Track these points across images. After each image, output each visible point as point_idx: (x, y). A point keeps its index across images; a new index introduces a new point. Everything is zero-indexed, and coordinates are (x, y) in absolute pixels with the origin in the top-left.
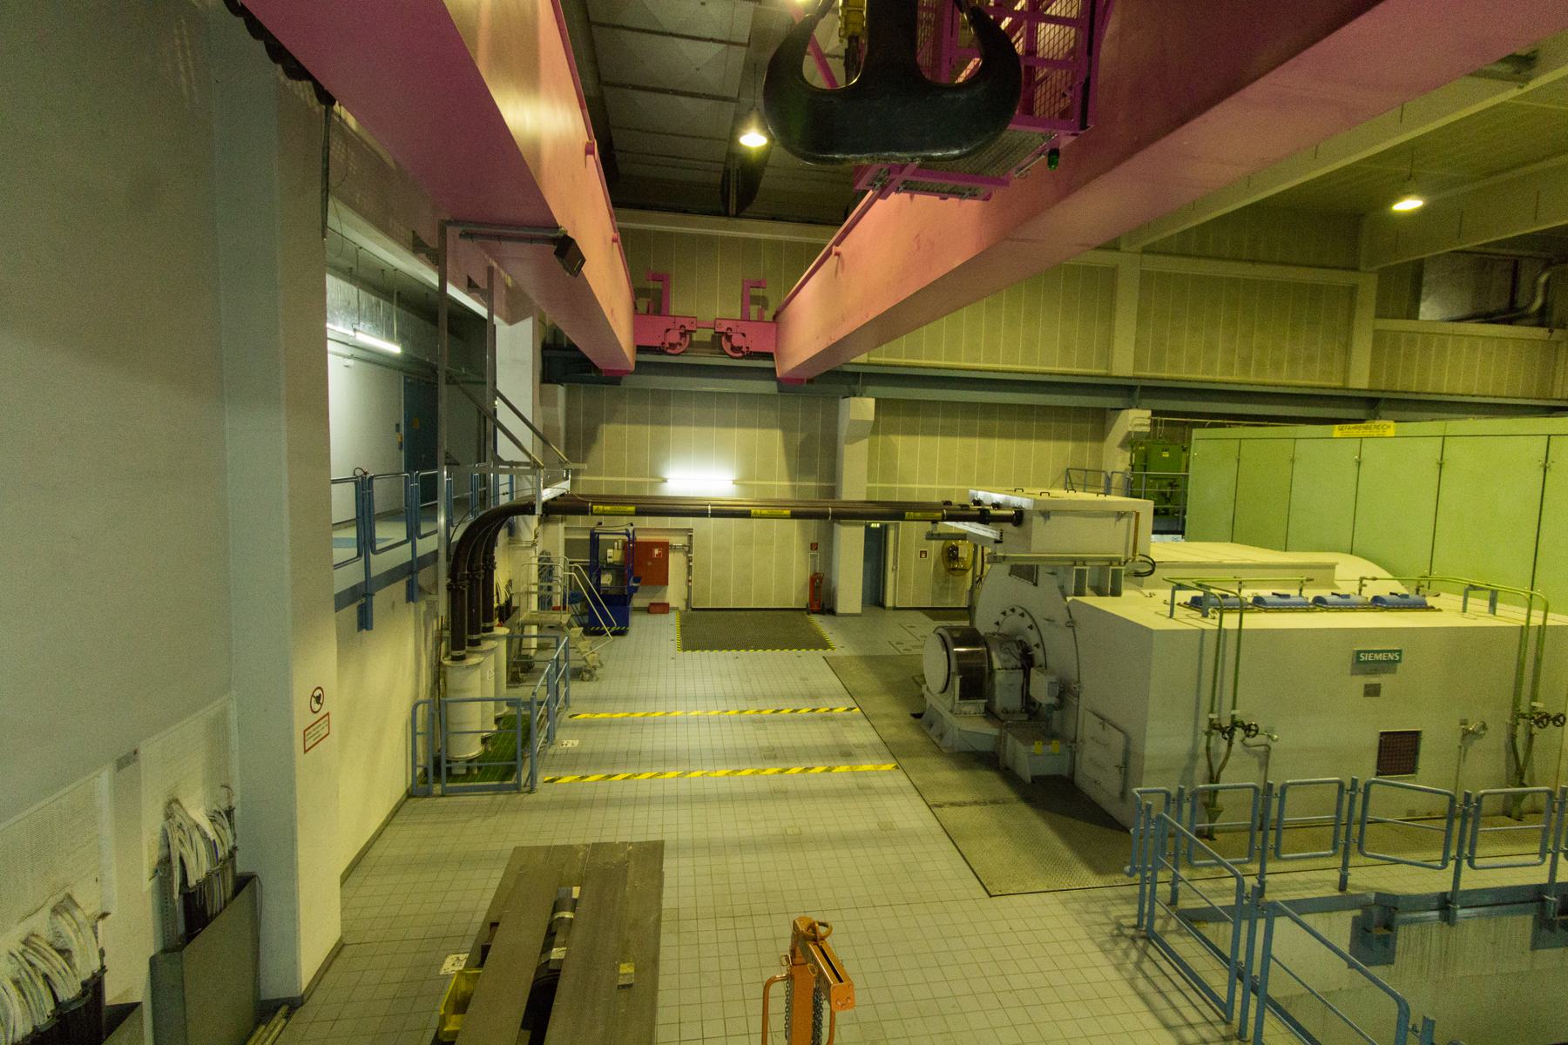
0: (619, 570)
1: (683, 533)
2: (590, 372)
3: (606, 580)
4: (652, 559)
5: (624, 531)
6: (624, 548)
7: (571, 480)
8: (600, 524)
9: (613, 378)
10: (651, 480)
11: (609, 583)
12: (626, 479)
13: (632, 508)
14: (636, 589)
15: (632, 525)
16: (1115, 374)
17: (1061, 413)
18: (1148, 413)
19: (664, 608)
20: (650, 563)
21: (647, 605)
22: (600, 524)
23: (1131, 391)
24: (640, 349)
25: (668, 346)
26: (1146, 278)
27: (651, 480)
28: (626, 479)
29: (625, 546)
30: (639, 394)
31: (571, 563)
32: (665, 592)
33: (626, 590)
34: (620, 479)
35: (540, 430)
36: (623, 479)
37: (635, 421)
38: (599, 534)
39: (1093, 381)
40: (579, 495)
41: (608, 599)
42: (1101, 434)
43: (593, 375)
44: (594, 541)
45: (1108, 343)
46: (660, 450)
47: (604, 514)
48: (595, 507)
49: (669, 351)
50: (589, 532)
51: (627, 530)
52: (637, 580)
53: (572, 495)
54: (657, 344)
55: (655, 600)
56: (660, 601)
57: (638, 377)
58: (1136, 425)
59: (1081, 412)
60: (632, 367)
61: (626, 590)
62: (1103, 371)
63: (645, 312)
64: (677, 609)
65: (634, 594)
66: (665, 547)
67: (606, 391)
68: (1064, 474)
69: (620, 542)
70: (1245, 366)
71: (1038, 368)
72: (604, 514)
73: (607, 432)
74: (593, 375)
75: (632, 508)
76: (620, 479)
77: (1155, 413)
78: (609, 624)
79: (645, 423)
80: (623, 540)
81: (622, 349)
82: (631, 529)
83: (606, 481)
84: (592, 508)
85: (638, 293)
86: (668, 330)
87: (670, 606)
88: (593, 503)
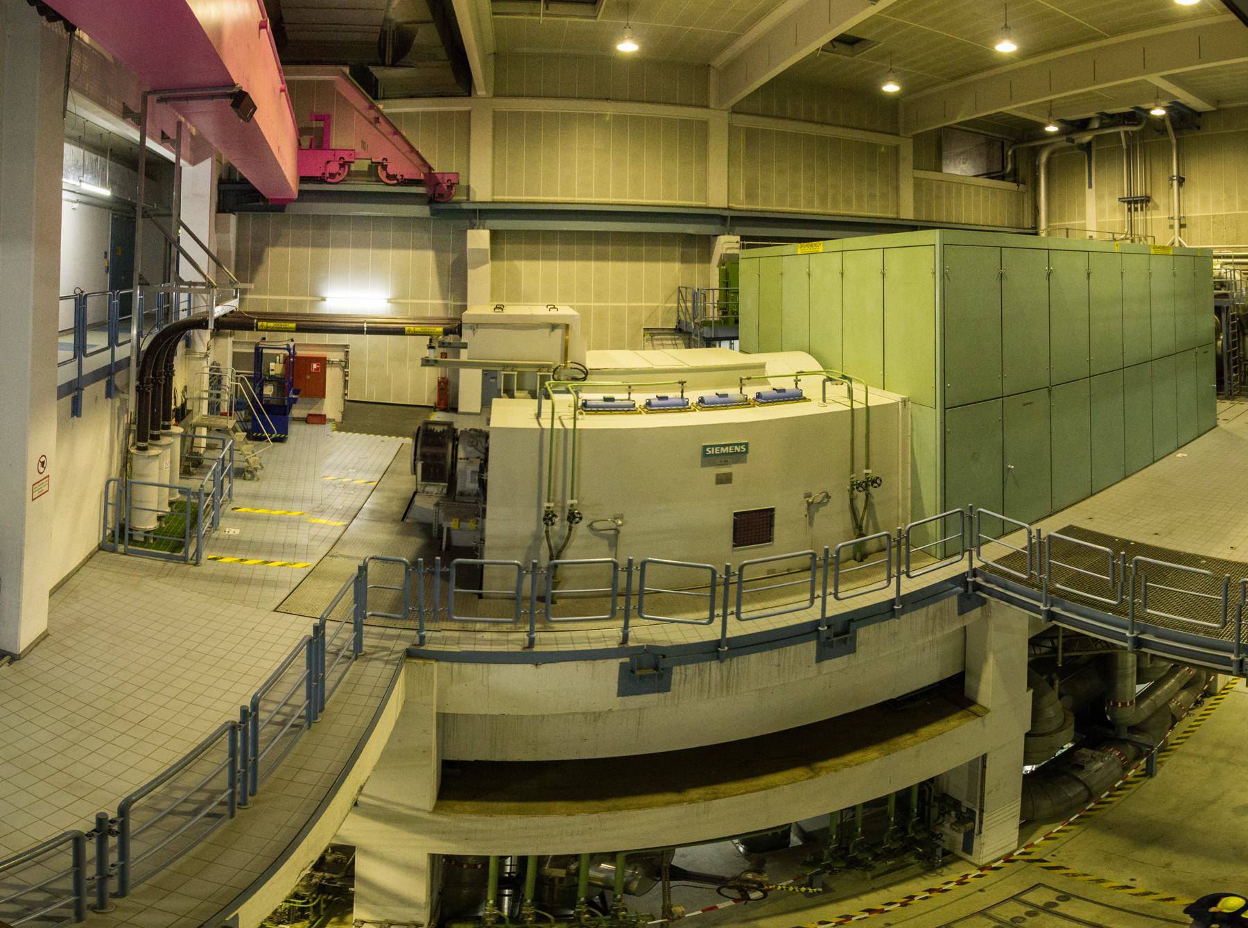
0: (279, 382)
1: (340, 349)
2: (258, 201)
3: (269, 390)
4: (311, 373)
5: (285, 347)
6: (284, 363)
7: (240, 299)
8: (264, 339)
9: (279, 206)
10: (311, 298)
11: (270, 393)
12: (288, 298)
13: (293, 325)
14: (295, 400)
15: (292, 340)
16: (711, 205)
17: (666, 239)
18: (738, 238)
19: (321, 419)
20: (308, 377)
21: (305, 416)
22: (264, 339)
23: (727, 220)
24: (303, 180)
25: (328, 175)
26: (732, 131)
27: (311, 298)
28: (288, 298)
29: (286, 359)
30: (302, 220)
31: (237, 374)
32: (323, 404)
33: (286, 401)
34: (282, 298)
35: (215, 254)
36: (285, 298)
37: (297, 244)
38: (263, 348)
39: (691, 211)
40: (246, 313)
41: (269, 408)
42: (706, 257)
43: (261, 204)
44: (258, 354)
45: (704, 180)
46: (319, 269)
47: (268, 330)
48: (260, 324)
49: (329, 180)
50: (254, 346)
51: (288, 345)
52: (296, 392)
53: (240, 312)
54: (319, 174)
55: (313, 412)
56: (318, 412)
57: (301, 204)
58: (728, 249)
59: (688, 239)
60: (296, 196)
61: (286, 401)
62: (703, 203)
63: (308, 147)
64: (333, 420)
65: (294, 405)
66: (323, 362)
67: (272, 217)
68: (677, 292)
69: (282, 356)
70: (810, 202)
71: (644, 201)
72: (268, 330)
73: (273, 255)
74: (261, 204)
75: (293, 325)
76: (282, 298)
77: (743, 238)
78: (270, 431)
79: (307, 246)
80: (285, 355)
81: (286, 180)
82: (291, 345)
83: (270, 300)
84: (257, 324)
85: (301, 131)
86: (328, 162)
87: (327, 417)
88: (259, 320)
